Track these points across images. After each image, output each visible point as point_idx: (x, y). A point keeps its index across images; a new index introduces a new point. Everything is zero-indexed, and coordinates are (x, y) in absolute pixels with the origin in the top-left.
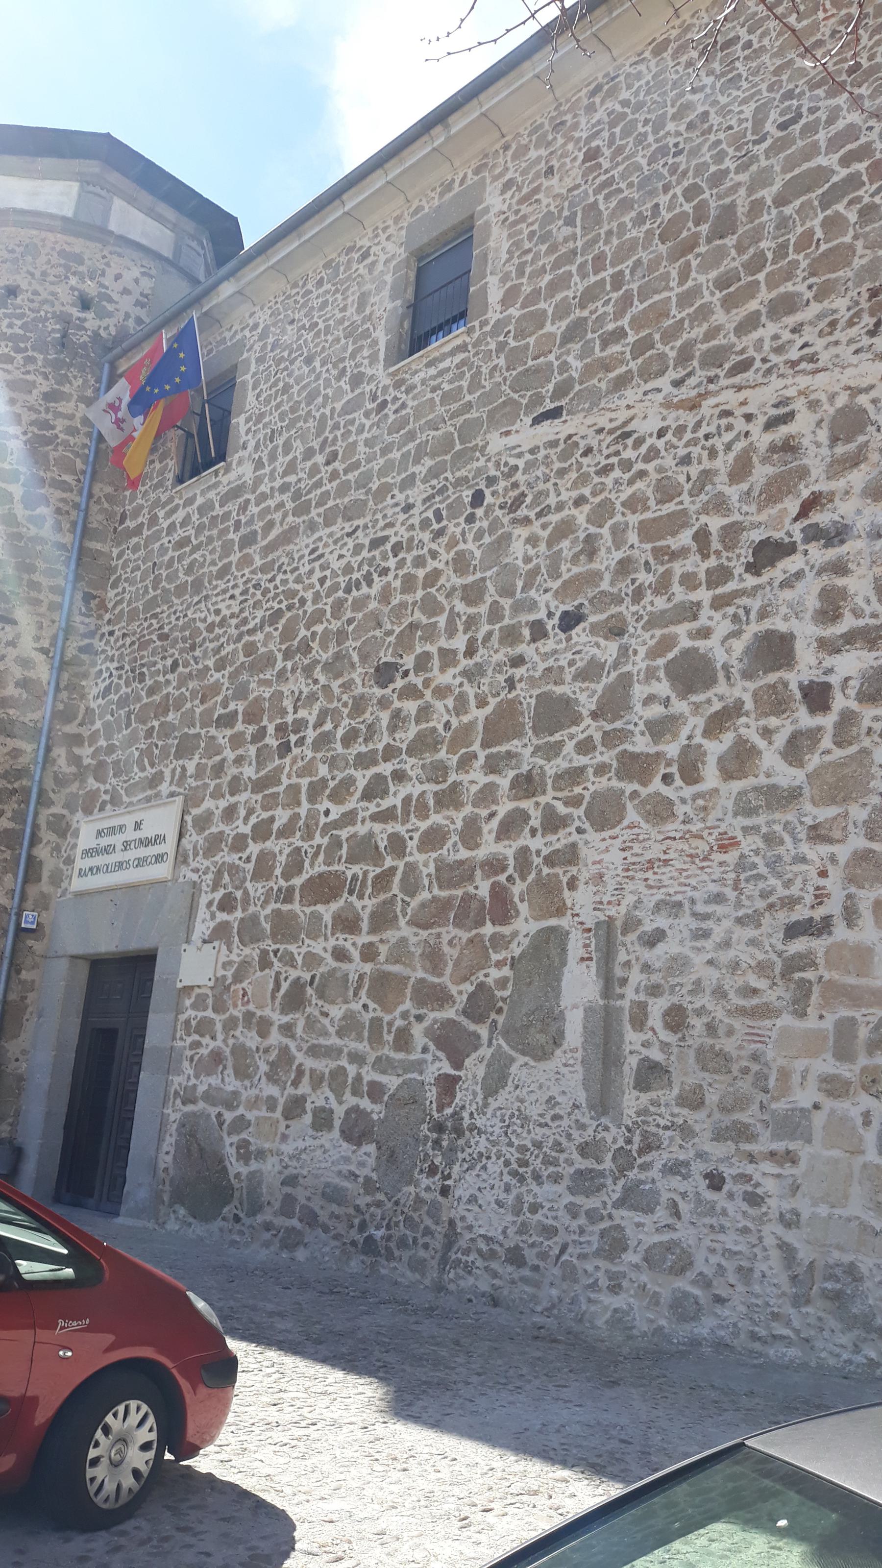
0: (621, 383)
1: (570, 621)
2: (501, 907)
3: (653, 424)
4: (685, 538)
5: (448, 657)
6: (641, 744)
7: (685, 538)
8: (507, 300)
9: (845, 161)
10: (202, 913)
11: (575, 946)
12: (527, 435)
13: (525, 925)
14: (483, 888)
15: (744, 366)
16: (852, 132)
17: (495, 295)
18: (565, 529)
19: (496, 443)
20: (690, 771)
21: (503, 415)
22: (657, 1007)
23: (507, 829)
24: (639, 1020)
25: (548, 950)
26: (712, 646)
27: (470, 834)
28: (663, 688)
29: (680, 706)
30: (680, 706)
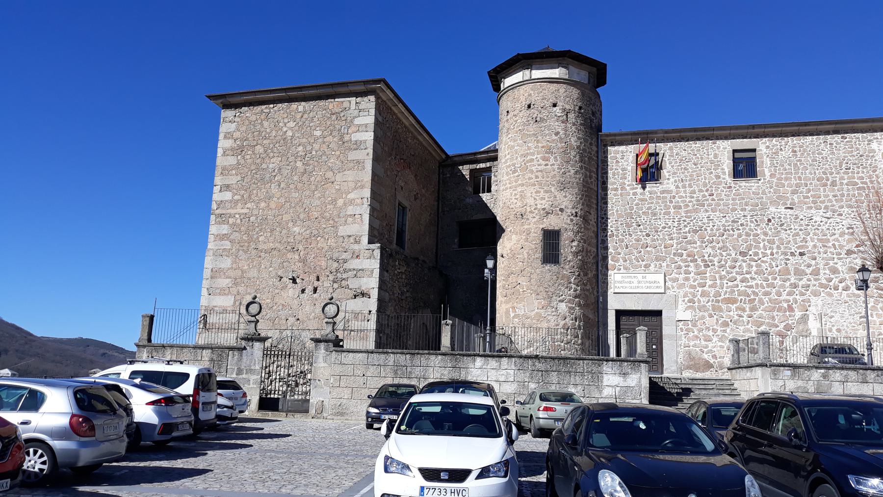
0: (811, 208)
1: (801, 254)
2: (790, 308)
3: (818, 219)
4: (830, 244)
5: (765, 255)
6: (824, 282)
7: (830, 244)
8: (772, 176)
9: (862, 183)
10: (680, 302)
11: (811, 318)
12: (782, 209)
13: (798, 314)
14: (785, 305)
15: (841, 215)
16: (862, 178)
17: (767, 174)
18: (797, 234)
19: (773, 209)
20: (836, 288)
21: (775, 203)
22: (834, 329)
23: (789, 294)
24: (830, 330)
25: (804, 319)
26: (838, 266)
27: (779, 294)
28: (827, 272)
29: (832, 276)
30: (832, 276)
